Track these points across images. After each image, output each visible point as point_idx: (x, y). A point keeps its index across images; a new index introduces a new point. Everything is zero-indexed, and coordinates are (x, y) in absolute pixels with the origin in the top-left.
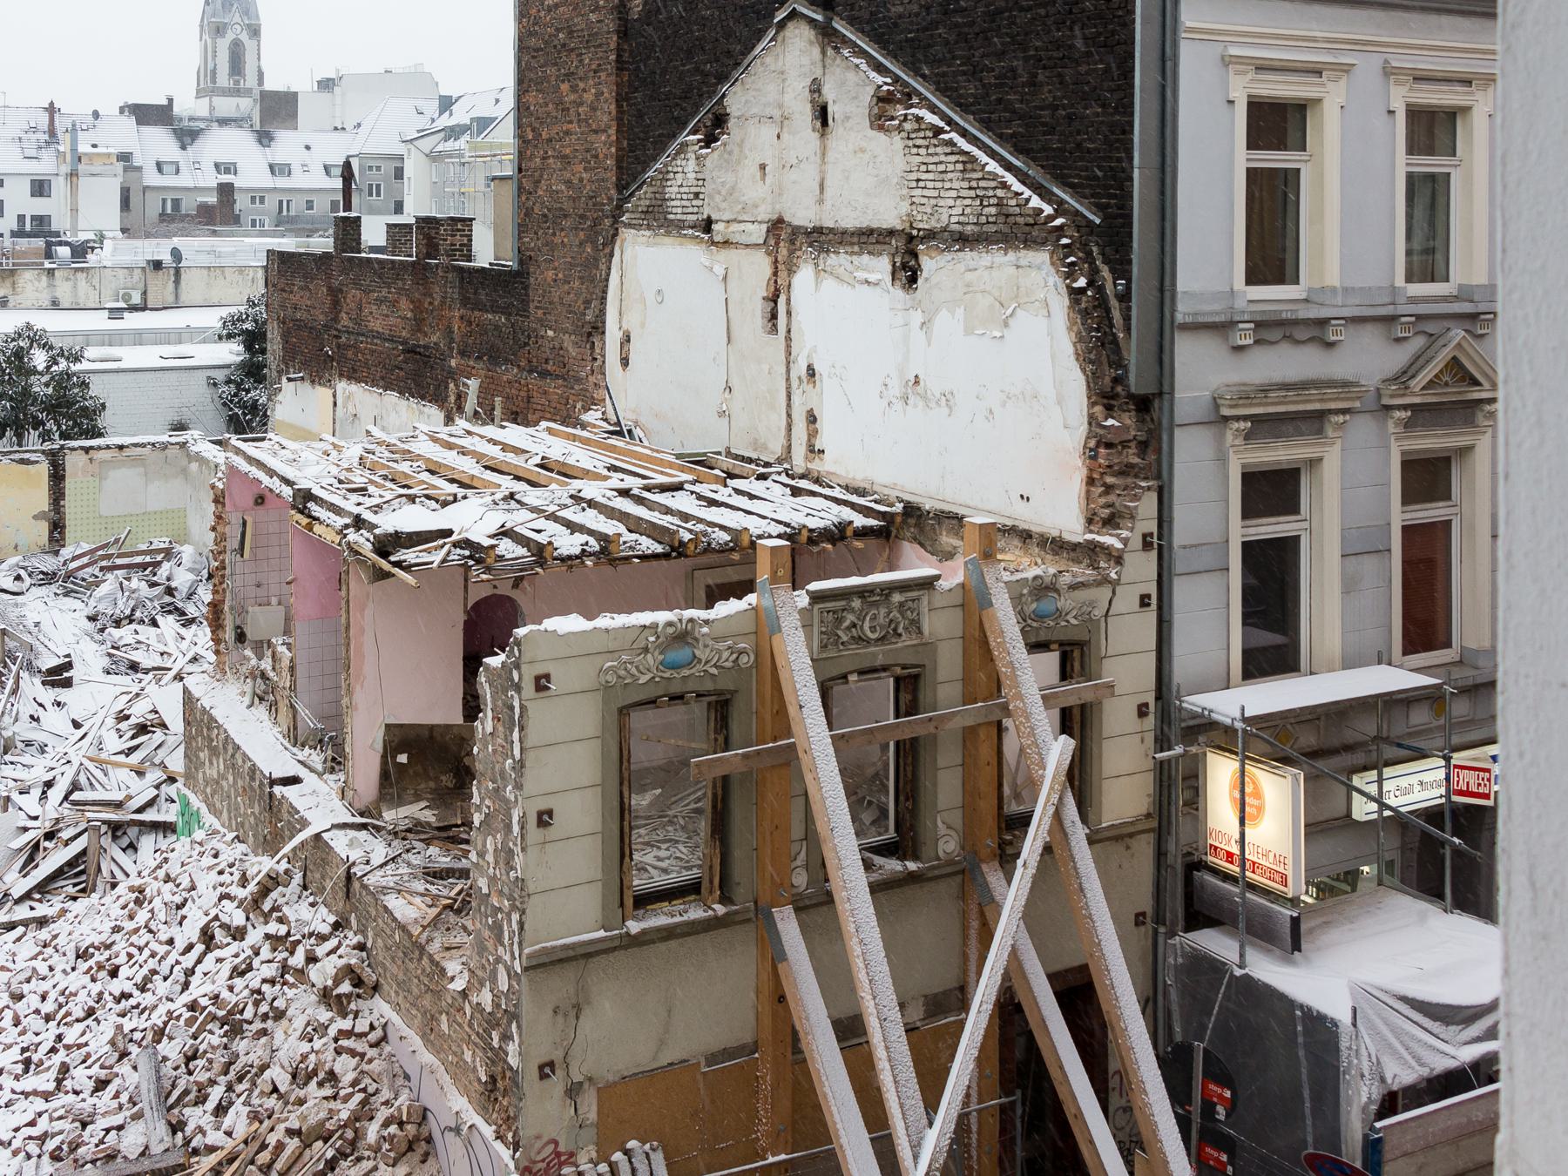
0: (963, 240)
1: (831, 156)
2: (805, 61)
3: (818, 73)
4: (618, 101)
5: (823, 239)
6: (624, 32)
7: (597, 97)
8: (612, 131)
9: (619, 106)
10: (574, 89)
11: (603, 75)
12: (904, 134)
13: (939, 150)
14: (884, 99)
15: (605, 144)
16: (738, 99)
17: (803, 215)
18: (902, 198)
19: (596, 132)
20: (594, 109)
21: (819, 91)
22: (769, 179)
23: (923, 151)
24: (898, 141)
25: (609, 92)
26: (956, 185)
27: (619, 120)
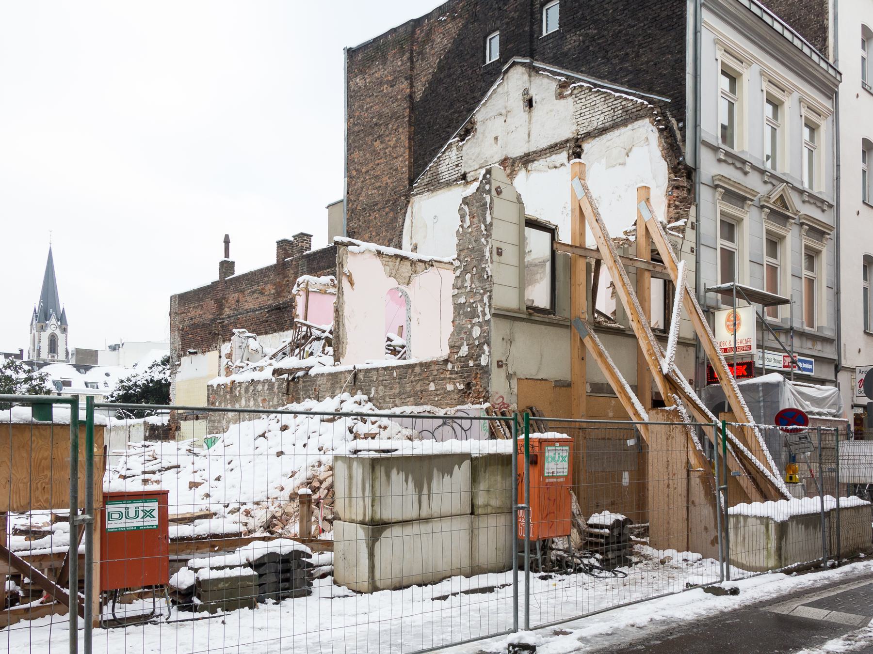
0: (603, 131)
1: (533, 120)
2: (520, 83)
3: (527, 86)
4: (410, 139)
5: (527, 159)
6: (413, 107)
7: (398, 143)
8: (407, 154)
9: (410, 142)
10: (382, 143)
11: (401, 130)
12: (574, 96)
13: (592, 96)
14: (563, 86)
15: (402, 163)
16: (481, 114)
17: (517, 151)
18: (573, 124)
19: (396, 158)
20: (395, 147)
21: (527, 94)
22: (499, 143)
23: (583, 100)
24: (570, 100)
25: (404, 138)
26: (601, 108)
27: (410, 148)
